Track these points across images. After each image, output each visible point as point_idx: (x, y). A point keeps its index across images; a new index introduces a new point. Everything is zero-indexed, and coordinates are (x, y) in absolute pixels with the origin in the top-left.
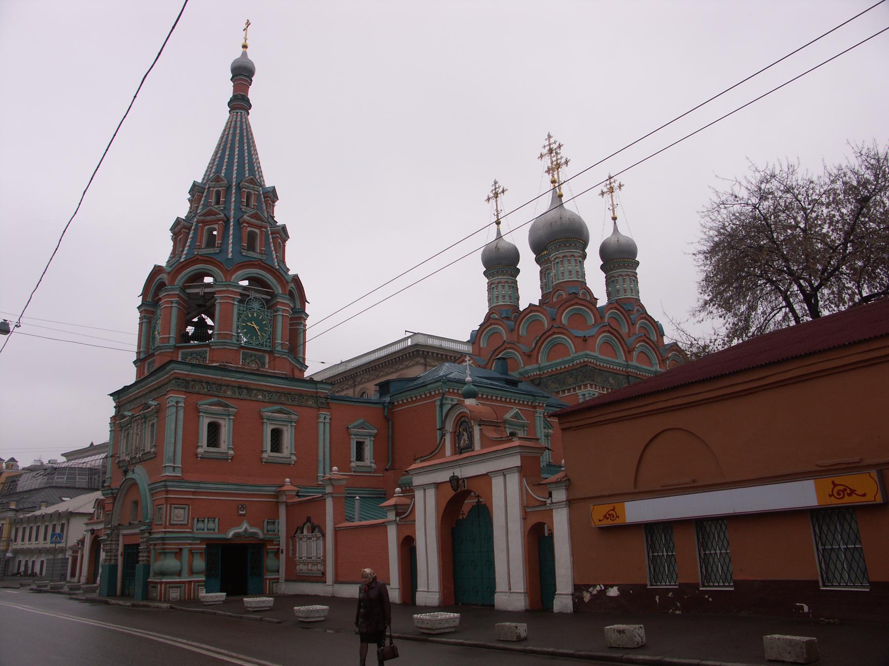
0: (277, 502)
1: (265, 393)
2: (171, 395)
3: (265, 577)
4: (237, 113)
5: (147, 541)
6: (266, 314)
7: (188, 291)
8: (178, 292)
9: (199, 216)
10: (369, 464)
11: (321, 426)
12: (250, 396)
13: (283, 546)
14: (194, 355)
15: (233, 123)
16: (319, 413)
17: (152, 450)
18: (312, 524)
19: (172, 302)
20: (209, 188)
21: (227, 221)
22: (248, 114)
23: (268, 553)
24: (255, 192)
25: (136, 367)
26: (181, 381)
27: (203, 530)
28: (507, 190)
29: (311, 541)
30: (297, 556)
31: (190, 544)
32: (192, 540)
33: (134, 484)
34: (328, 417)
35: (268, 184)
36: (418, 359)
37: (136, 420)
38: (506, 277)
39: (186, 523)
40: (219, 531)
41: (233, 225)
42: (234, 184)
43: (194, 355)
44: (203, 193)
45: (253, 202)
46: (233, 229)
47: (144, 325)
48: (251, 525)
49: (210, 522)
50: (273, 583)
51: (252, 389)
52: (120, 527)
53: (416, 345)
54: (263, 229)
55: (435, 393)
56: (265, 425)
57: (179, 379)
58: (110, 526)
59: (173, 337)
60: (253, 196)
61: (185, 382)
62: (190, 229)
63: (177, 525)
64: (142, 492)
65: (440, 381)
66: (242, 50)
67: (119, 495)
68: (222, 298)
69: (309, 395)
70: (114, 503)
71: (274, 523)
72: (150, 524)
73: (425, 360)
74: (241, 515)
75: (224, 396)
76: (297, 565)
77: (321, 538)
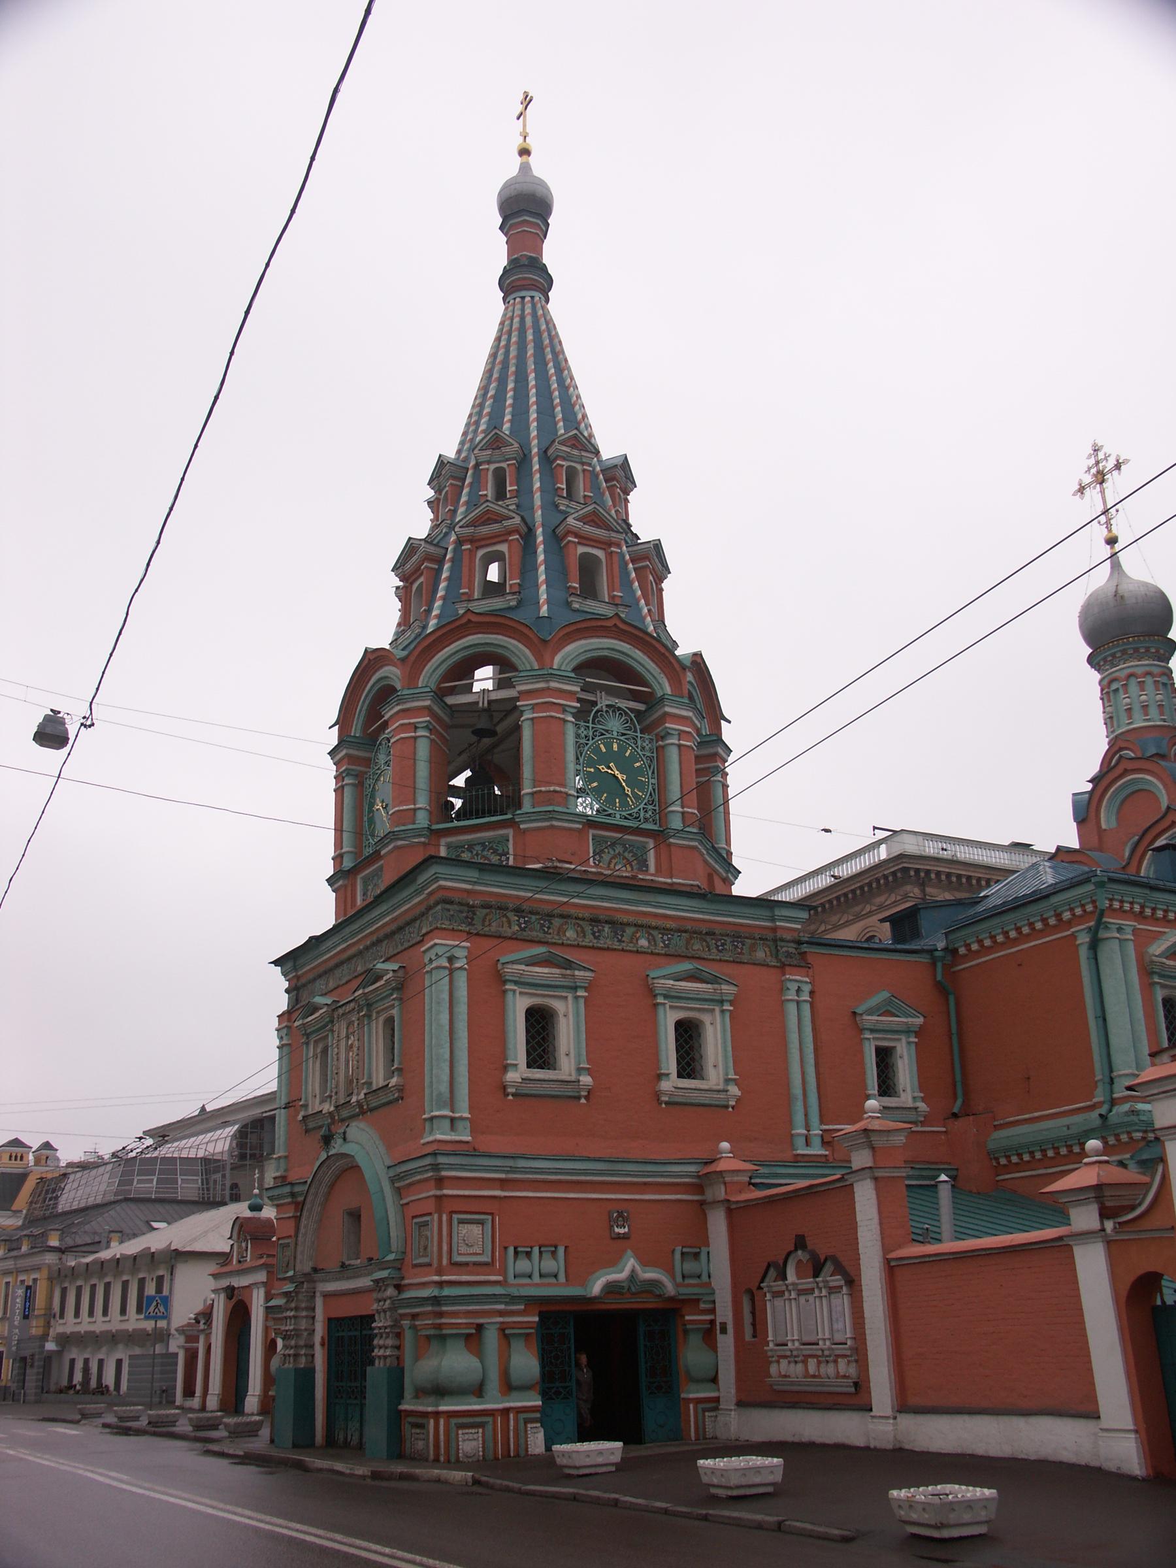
0: (702, 1203)
1: (655, 933)
2: (437, 941)
3: (683, 1395)
4: (523, 298)
5: (393, 1309)
6: (639, 743)
7: (450, 700)
8: (427, 703)
9: (460, 527)
10: (910, 1104)
11: (792, 1008)
12: (620, 941)
13: (725, 1312)
14: (478, 848)
15: (516, 320)
16: (783, 978)
17: (394, 1081)
18: (814, 1257)
19: (416, 728)
20: (477, 465)
21: (528, 535)
22: (547, 300)
23: (686, 1332)
24: (585, 467)
25: (333, 891)
26: (456, 907)
27: (530, 1277)
28: (1126, 461)
29: (811, 1298)
30: (770, 1338)
31: (501, 1313)
32: (506, 1303)
33: (350, 1169)
34: (807, 988)
35: (608, 451)
36: (908, 888)
37: (343, 1014)
38: (1147, 662)
39: (489, 1260)
40: (567, 1281)
41: (544, 542)
42: (535, 450)
43: (478, 848)
44: (464, 480)
45: (581, 490)
46: (545, 551)
47: (346, 789)
48: (644, 1263)
49: (544, 1255)
50: (704, 1410)
51: (621, 924)
52: (318, 1276)
53: (901, 857)
54: (612, 549)
55: (1074, 915)
56: (661, 1010)
57: (452, 903)
58: (291, 1273)
59: (425, 809)
60: (581, 475)
61: (466, 909)
62: (440, 561)
63: (467, 1264)
64: (372, 1187)
65: (1087, 881)
66: (518, 160)
67: (310, 1198)
68: (534, 707)
69: (757, 937)
70: (298, 1219)
71: (696, 1256)
72: (399, 1265)
73: (923, 891)
74: (620, 1237)
75: (560, 942)
76: (771, 1362)
77: (844, 1288)
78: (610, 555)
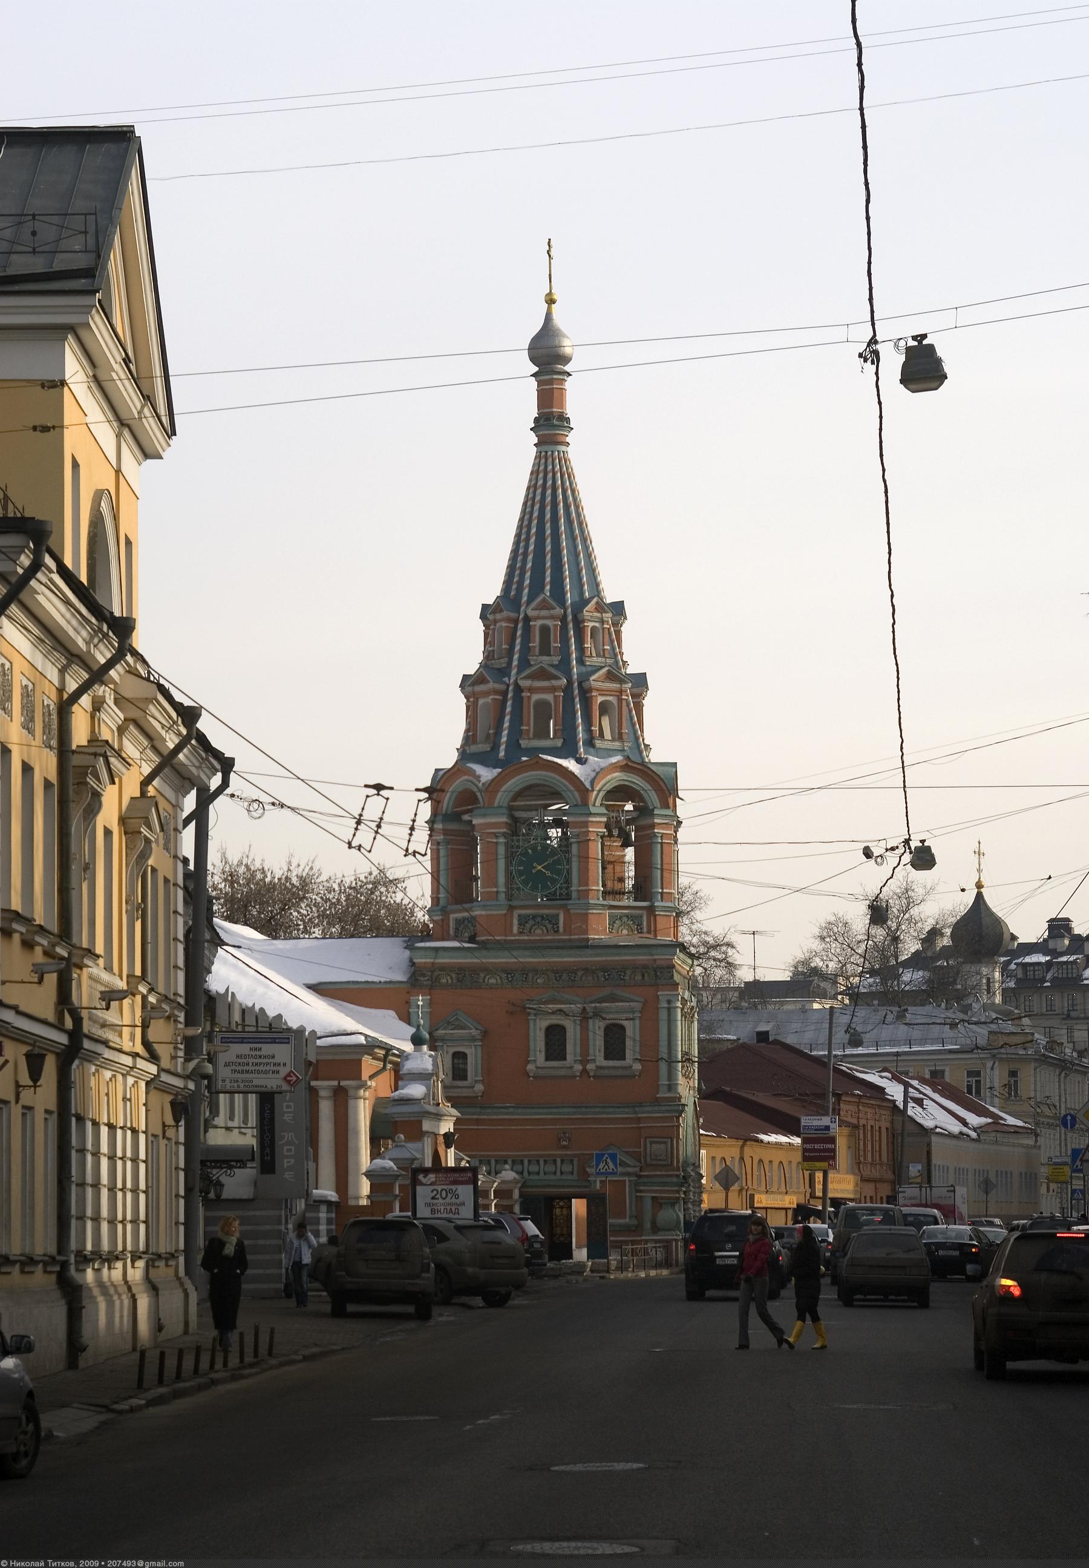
7: (518, 814)
14: (539, 919)
78: (620, 700)
